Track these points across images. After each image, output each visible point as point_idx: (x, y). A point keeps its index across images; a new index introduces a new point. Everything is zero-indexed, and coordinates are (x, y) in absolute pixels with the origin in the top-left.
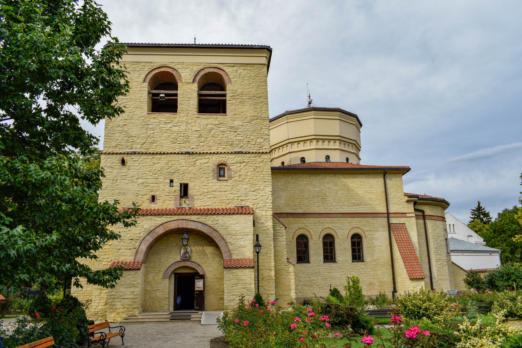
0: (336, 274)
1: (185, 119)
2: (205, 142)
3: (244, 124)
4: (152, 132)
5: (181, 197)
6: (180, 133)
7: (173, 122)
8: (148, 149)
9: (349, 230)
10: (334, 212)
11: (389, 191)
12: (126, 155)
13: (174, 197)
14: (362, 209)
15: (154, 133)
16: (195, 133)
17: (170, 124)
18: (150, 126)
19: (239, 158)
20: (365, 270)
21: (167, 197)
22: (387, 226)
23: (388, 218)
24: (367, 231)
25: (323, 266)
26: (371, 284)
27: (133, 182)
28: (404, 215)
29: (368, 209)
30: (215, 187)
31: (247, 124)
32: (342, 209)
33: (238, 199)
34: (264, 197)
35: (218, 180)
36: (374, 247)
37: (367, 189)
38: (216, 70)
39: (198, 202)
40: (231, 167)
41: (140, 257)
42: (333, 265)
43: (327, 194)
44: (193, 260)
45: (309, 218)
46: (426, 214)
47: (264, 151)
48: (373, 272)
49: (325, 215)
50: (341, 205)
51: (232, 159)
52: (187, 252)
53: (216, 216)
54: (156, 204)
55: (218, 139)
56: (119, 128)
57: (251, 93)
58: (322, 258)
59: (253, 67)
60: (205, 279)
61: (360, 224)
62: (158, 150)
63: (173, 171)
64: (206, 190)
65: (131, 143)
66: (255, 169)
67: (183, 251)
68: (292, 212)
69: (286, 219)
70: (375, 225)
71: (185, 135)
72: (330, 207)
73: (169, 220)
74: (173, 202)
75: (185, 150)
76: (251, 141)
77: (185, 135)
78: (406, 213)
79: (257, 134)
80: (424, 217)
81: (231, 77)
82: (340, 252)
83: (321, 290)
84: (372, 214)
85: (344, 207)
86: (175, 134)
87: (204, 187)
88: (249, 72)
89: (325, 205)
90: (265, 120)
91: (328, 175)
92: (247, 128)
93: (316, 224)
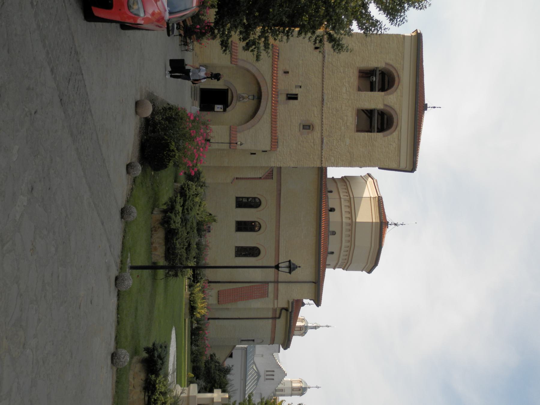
2: (332, 114)
4: (342, 71)
5: (287, 94)
6: (340, 94)
7: (350, 88)
10: (280, 232)
11: (298, 285)
15: (340, 72)
17: (348, 86)
18: (347, 70)
19: (318, 141)
22: (266, 281)
23: (274, 282)
31: (347, 149)
34: (285, 160)
35: (300, 124)
38: (395, 124)
40: (310, 135)
41: (240, 63)
44: (237, 103)
46: (277, 320)
52: (244, 98)
53: (270, 121)
57: (373, 153)
58: (239, 219)
60: (222, 113)
62: (326, 76)
67: (245, 95)
68: (282, 194)
71: (339, 98)
75: (325, 98)
76: (332, 152)
77: (339, 98)
78: (277, 299)
79: (338, 157)
80: (274, 318)
81: (389, 137)
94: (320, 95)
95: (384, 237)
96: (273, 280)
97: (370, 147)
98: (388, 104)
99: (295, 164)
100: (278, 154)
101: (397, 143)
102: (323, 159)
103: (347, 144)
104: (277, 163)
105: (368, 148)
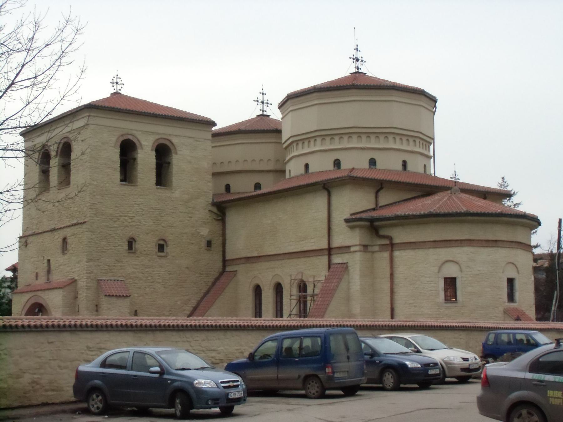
8: (38, 229)
23: (330, 255)
30: (62, 261)
46: (396, 241)
68: (249, 255)
78: (349, 247)
96: (325, 259)
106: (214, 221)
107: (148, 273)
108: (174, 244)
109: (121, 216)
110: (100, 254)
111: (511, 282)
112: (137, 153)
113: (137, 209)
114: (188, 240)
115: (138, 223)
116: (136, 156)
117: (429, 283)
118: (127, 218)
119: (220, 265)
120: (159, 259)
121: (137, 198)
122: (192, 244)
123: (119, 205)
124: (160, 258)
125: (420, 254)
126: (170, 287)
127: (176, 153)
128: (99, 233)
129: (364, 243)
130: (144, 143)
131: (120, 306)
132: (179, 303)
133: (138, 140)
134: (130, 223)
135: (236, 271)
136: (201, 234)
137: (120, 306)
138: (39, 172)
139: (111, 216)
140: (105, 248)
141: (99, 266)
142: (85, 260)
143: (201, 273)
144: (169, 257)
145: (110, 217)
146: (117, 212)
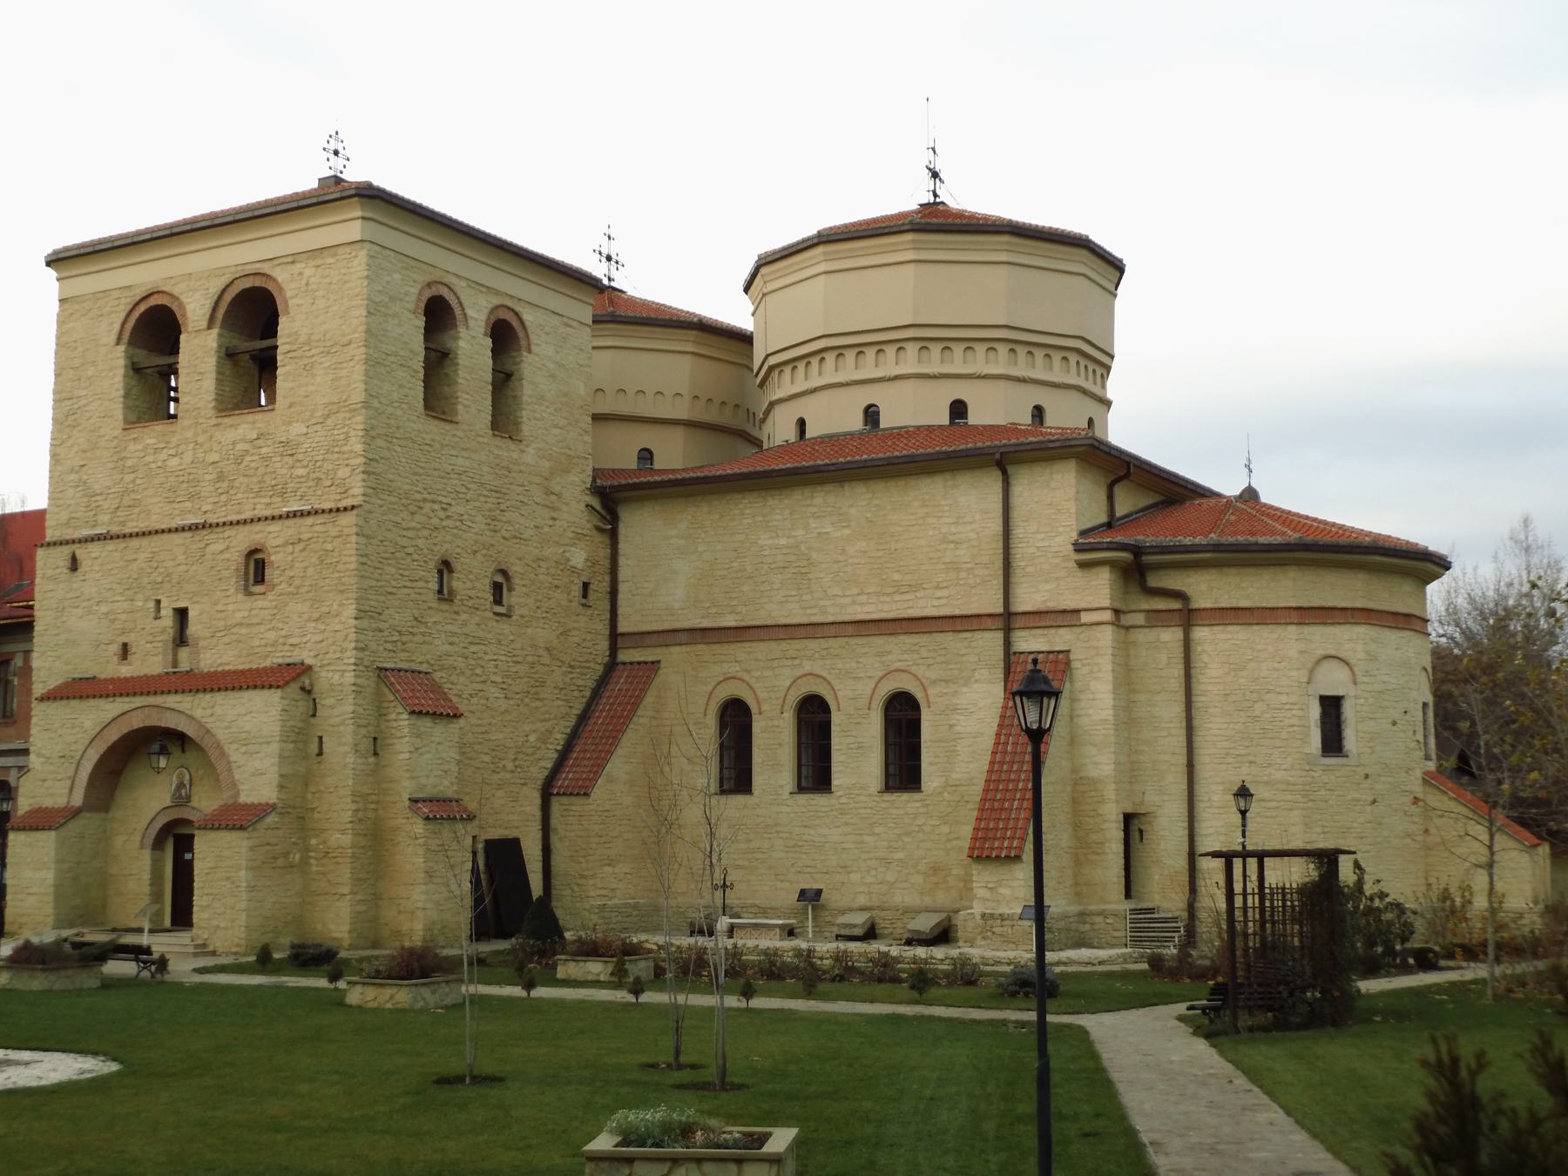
0: (826, 831)
1: (189, 434)
3: (310, 430)
6: (181, 473)
7: (170, 446)
8: (123, 524)
9: (877, 679)
10: (830, 619)
11: (1018, 532)
12: (78, 545)
13: (161, 644)
14: (886, 607)
15: (134, 481)
16: (210, 469)
17: (165, 451)
18: (129, 463)
20: (920, 821)
21: (149, 645)
23: (1008, 631)
24: (934, 682)
25: (789, 803)
26: (935, 869)
27: (90, 613)
28: (1068, 619)
29: (944, 601)
30: (241, 614)
32: (859, 608)
33: (285, 644)
36: (954, 740)
37: (945, 529)
39: (208, 655)
42: (819, 800)
43: (814, 555)
45: (754, 644)
47: (348, 502)
48: (946, 829)
49: (803, 632)
50: (856, 591)
51: (276, 535)
54: (130, 664)
55: (255, 479)
56: (72, 476)
57: (327, 337)
59: (335, 255)
61: (916, 656)
62: (143, 525)
63: (159, 580)
64: (222, 623)
65: (93, 513)
66: (323, 557)
68: (705, 624)
69: (689, 648)
70: (964, 659)
71: (192, 477)
72: (821, 603)
73: (127, 707)
74: (160, 657)
77: (192, 477)
78: (1078, 611)
79: (336, 456)
82: (842, 758)
83: (779, 885)
84: (959, 621)
85: (863, 598)
86: (172, 479)
87: (219, 615)
88: (326, 272)
89: (804, 597)
90: (355, 410)
91: (819, 489)
92: (316, 440)
93: (775, 664)
94: (177, 538)
95: (986, 218)
96: (998, 637)
97: (313, 352)
98: (208, 316)
99: (347, 599)
100: (322, 660)
101: (303, 265)
102: (341, 505)
103: (304, 430)
104: (345, 661)
105: (314, 359)
106: (595, 532)
107: (475, 656)
108: (524, 586)
109: (425, 500)
110: (383, 598)
111: (1331, 707)
112: (457, 338)
113: (456, 485)
114: (550, 579)
115: (458, 523)
116: (450, 344)
117: (1287, 707)
118: (436, 507)
119: (604, 645)
120: (497, 621)
121: (457, 456)
122: (556, 587)
123: (422, 471)
124: (498, 618)
125: (1265, 636)
126: (517, 696)
127: (529, 351)
128: (382, 541)
129: (1117, 605)
130: (470, 312)
131: (439, 743)
132: (532, 738)
133: (461, 304)
134: (442, 520)
135: (659, 662)
136: (571, 563)
137: (439, 743)
138: (126, 366)
139: (407, 498)
140: (393, 583)
141: (381, 631)
142: (351, 610)
143: (572, 663)
144: (514, 618)
145: (404, 501)
146: (417, 489)
